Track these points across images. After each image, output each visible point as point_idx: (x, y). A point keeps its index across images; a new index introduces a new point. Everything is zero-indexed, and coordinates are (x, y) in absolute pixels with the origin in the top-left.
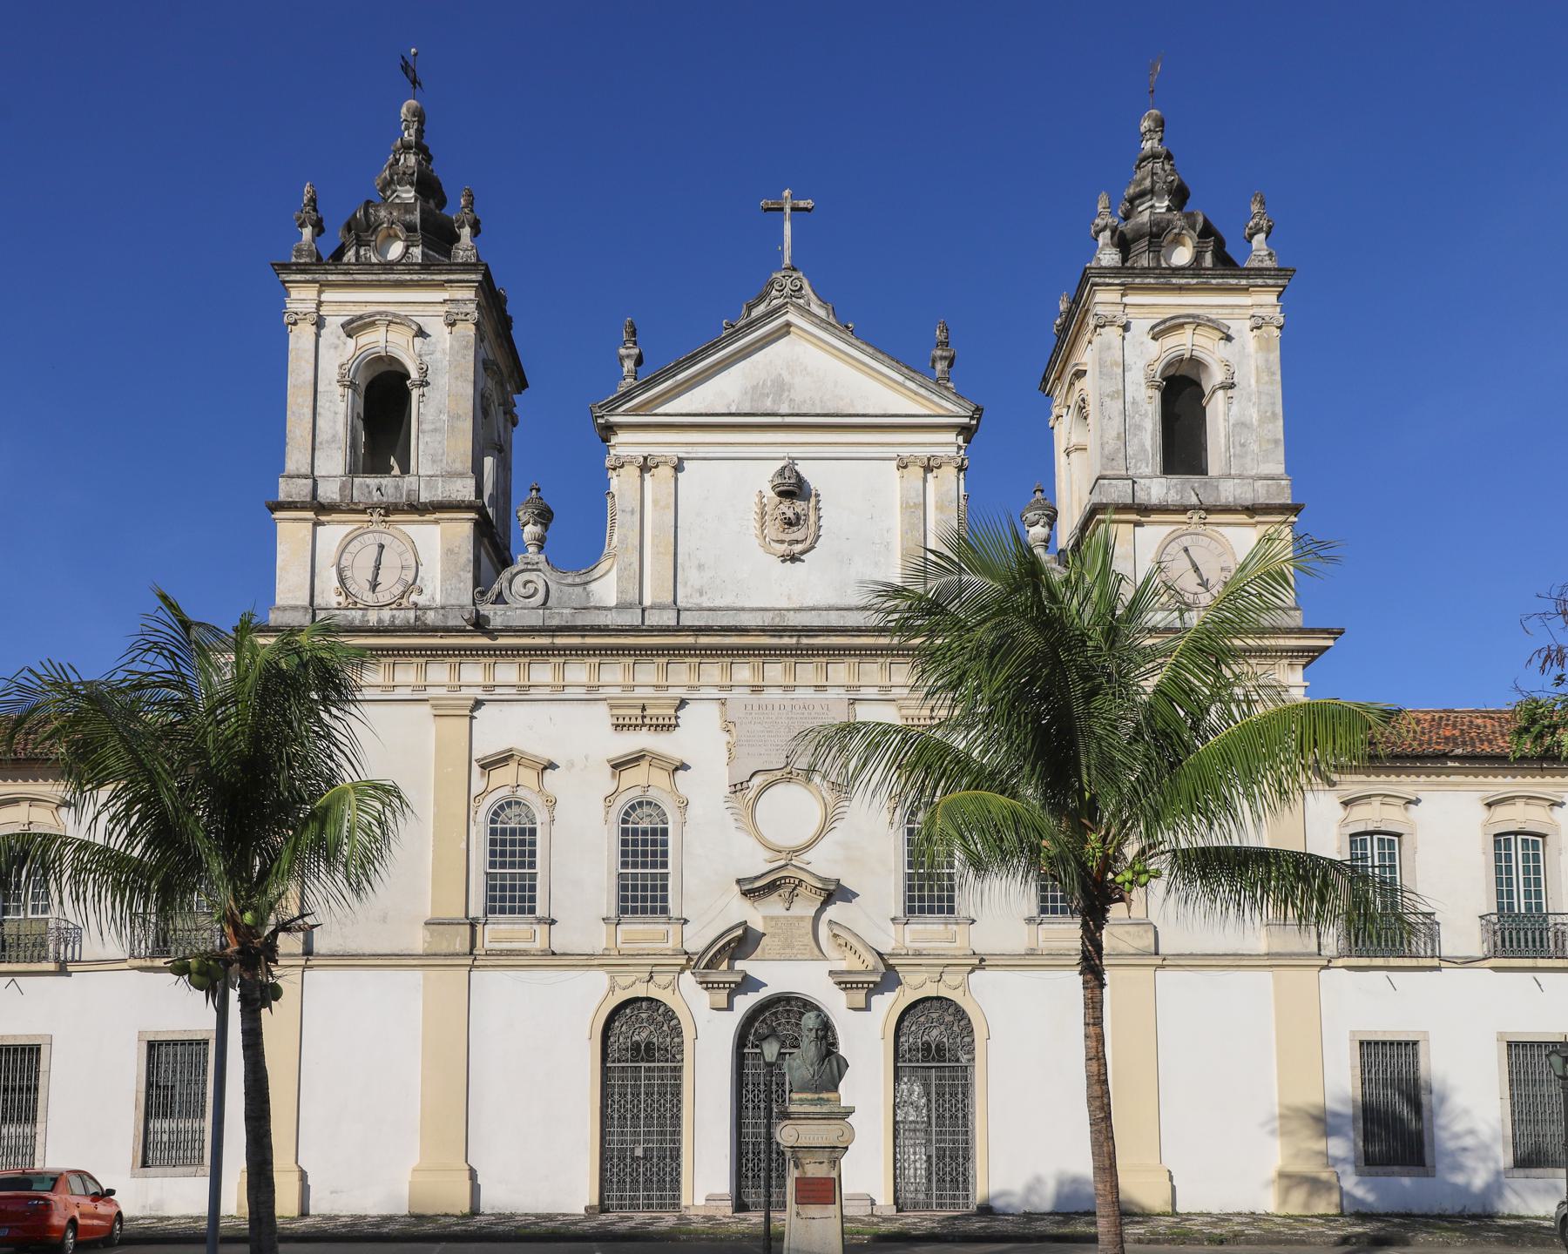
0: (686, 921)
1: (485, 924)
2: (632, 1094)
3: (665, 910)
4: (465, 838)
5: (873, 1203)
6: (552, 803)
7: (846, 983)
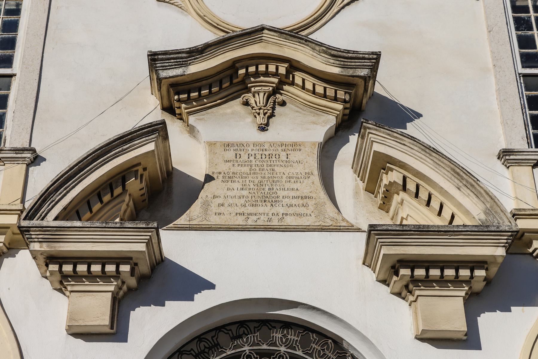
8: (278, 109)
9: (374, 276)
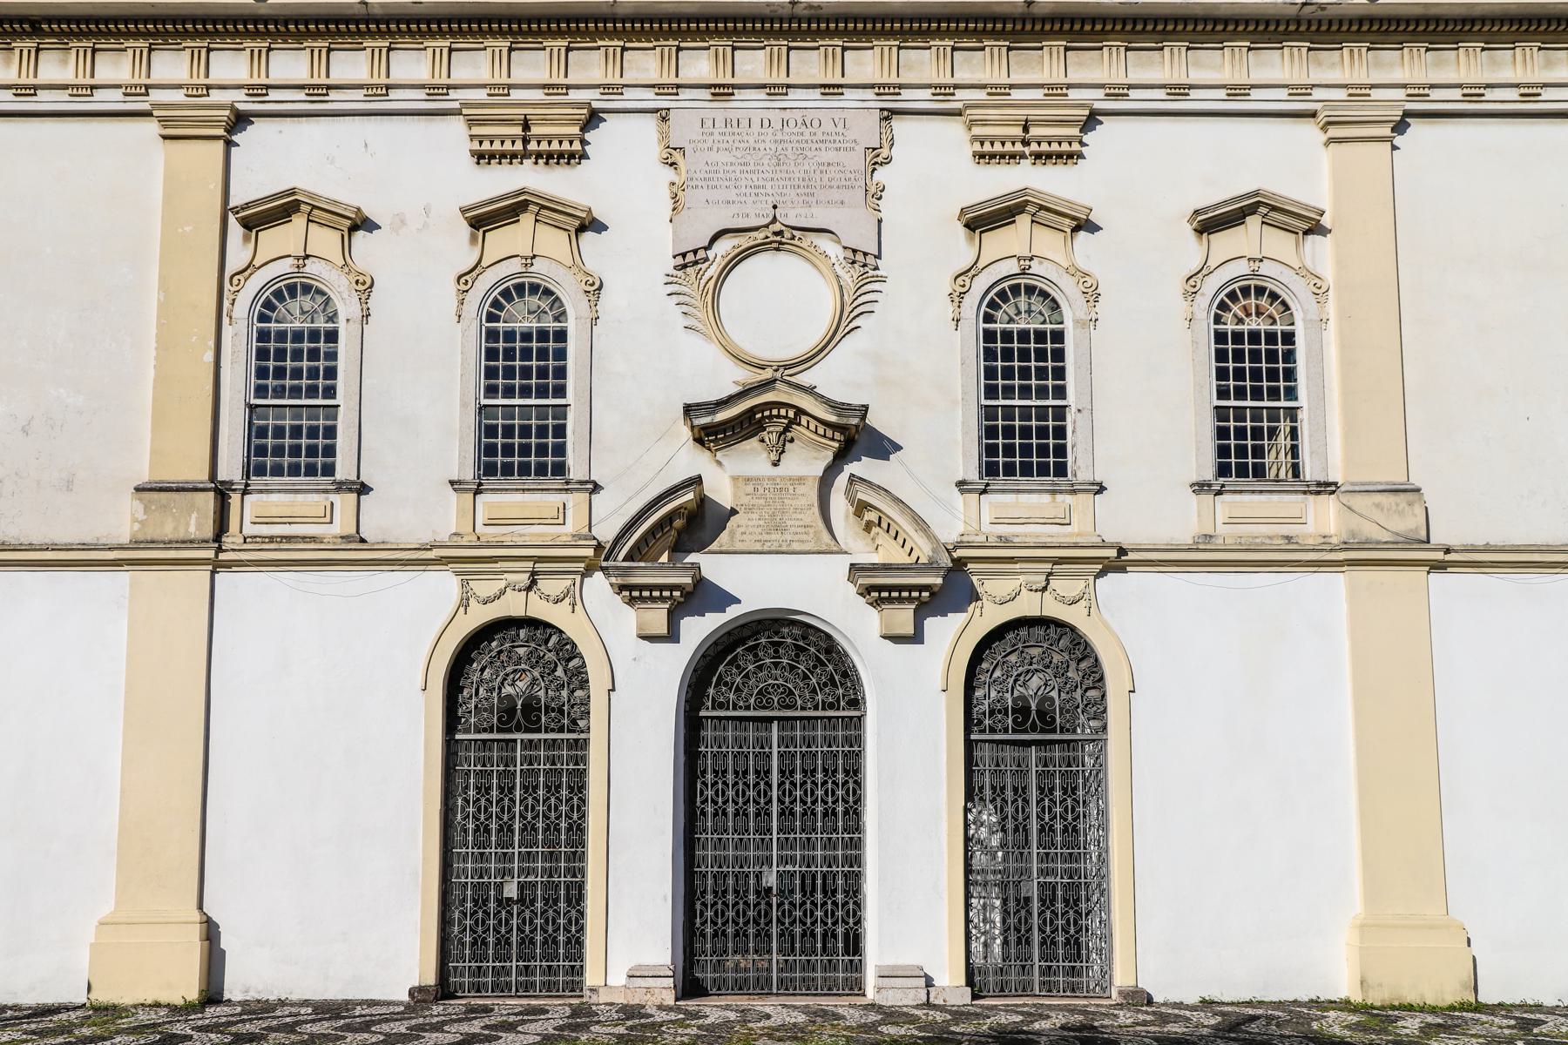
0: (596, 488)
1: (245, 492)
3: (560, 469)
4: (212, 343)
5: (929, 983)
6: (365, 287)
7: (880, 588)
8: (788, 445)
9: (855, 590)
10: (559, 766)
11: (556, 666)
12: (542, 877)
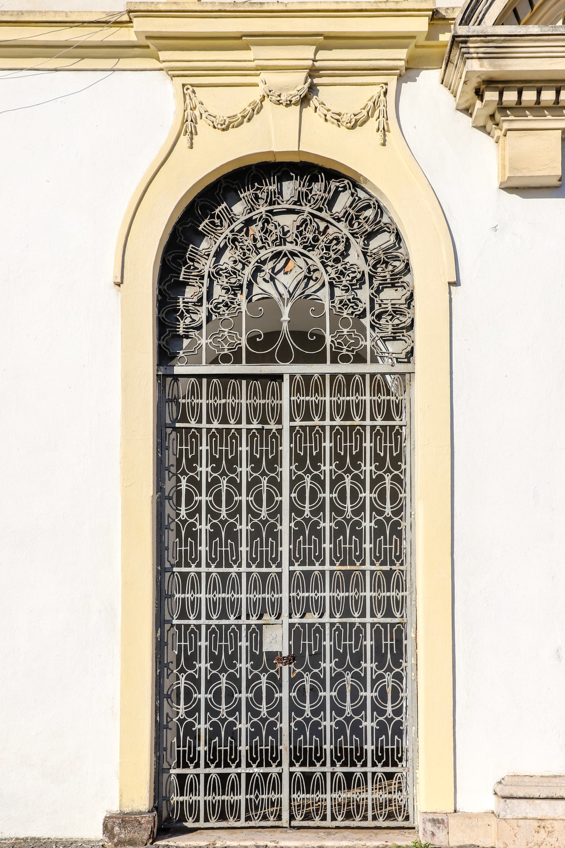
2: (255, 463)
10: (357, 421)
11: (348, 246)
12: (332, 616)
